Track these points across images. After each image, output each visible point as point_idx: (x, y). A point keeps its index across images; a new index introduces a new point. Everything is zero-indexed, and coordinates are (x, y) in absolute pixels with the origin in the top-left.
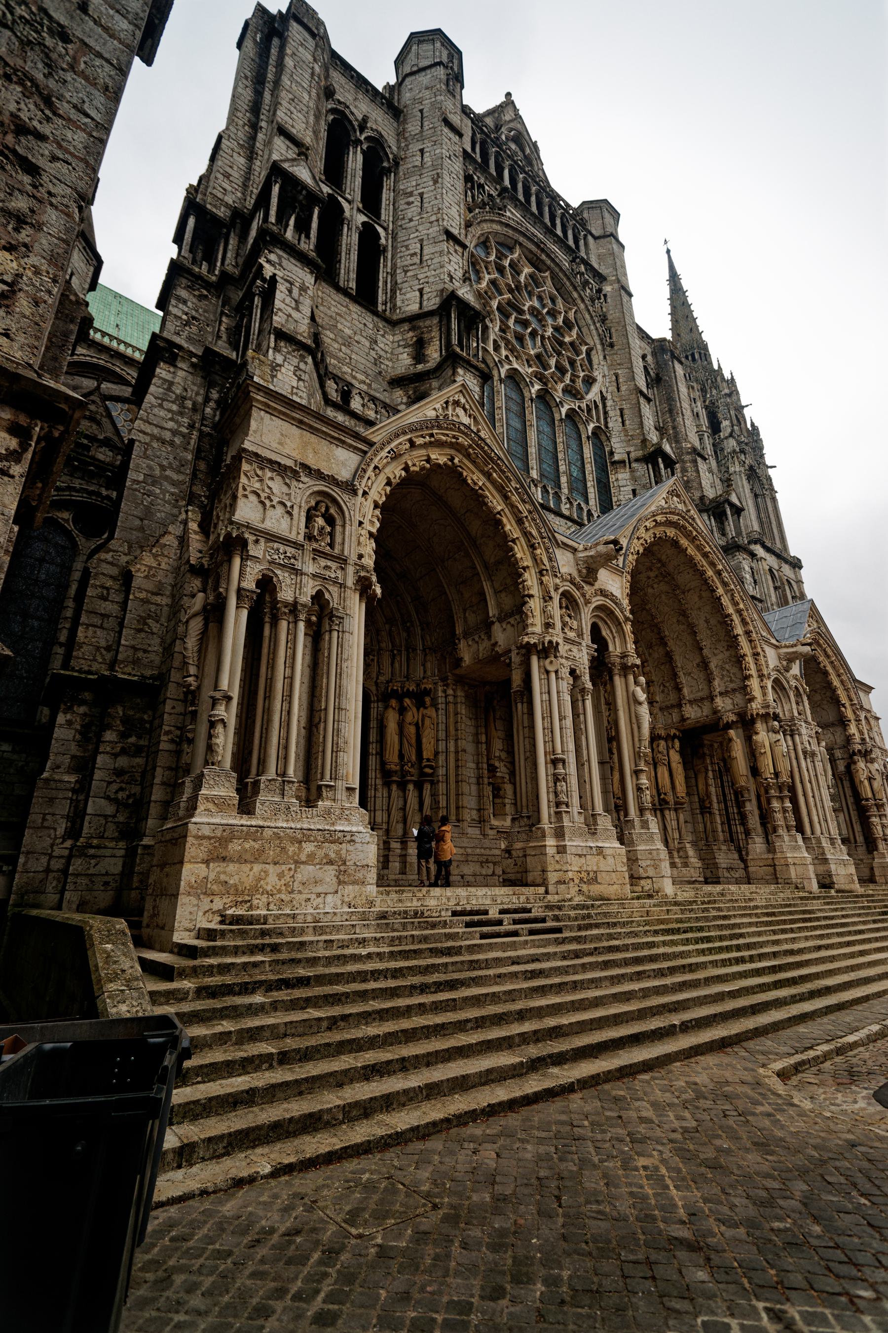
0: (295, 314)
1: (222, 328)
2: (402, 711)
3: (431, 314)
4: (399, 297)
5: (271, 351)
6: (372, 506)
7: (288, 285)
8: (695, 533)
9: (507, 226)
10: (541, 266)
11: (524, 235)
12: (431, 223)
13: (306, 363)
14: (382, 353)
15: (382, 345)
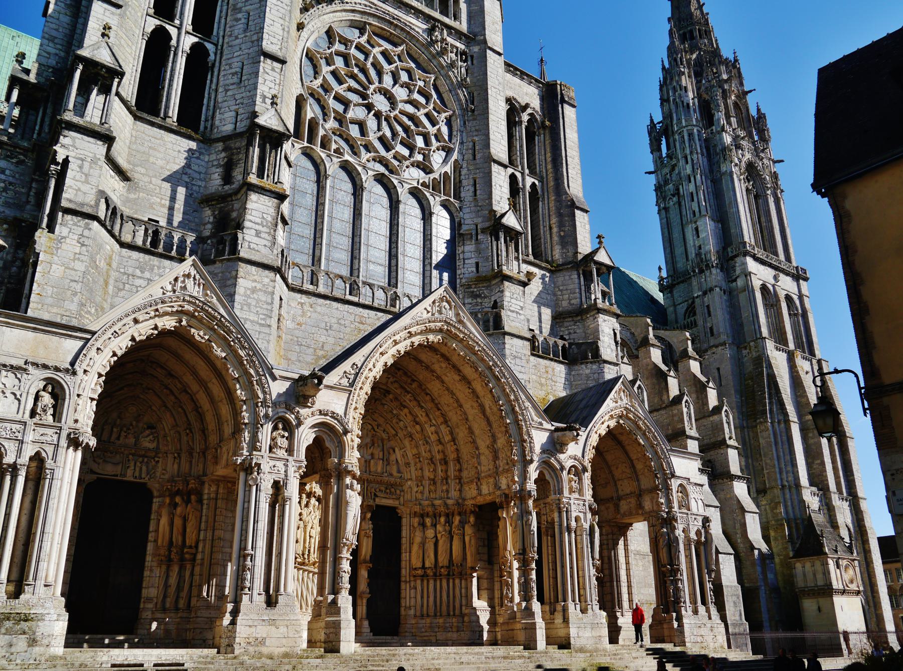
0: (85, 188)
1: (32, 193)
2: (175, 505)
3: (241, 135)
4: (218, 116)
5: (58, 226)
6: (97, 376)
7: (80, 162)
8: (462, 336)
9: (353, 11)
10: (396, 40)
11: (374, 16)
12: (252, 42)
13: (90, 229)
14: (196, 176)
15: (195, 167)
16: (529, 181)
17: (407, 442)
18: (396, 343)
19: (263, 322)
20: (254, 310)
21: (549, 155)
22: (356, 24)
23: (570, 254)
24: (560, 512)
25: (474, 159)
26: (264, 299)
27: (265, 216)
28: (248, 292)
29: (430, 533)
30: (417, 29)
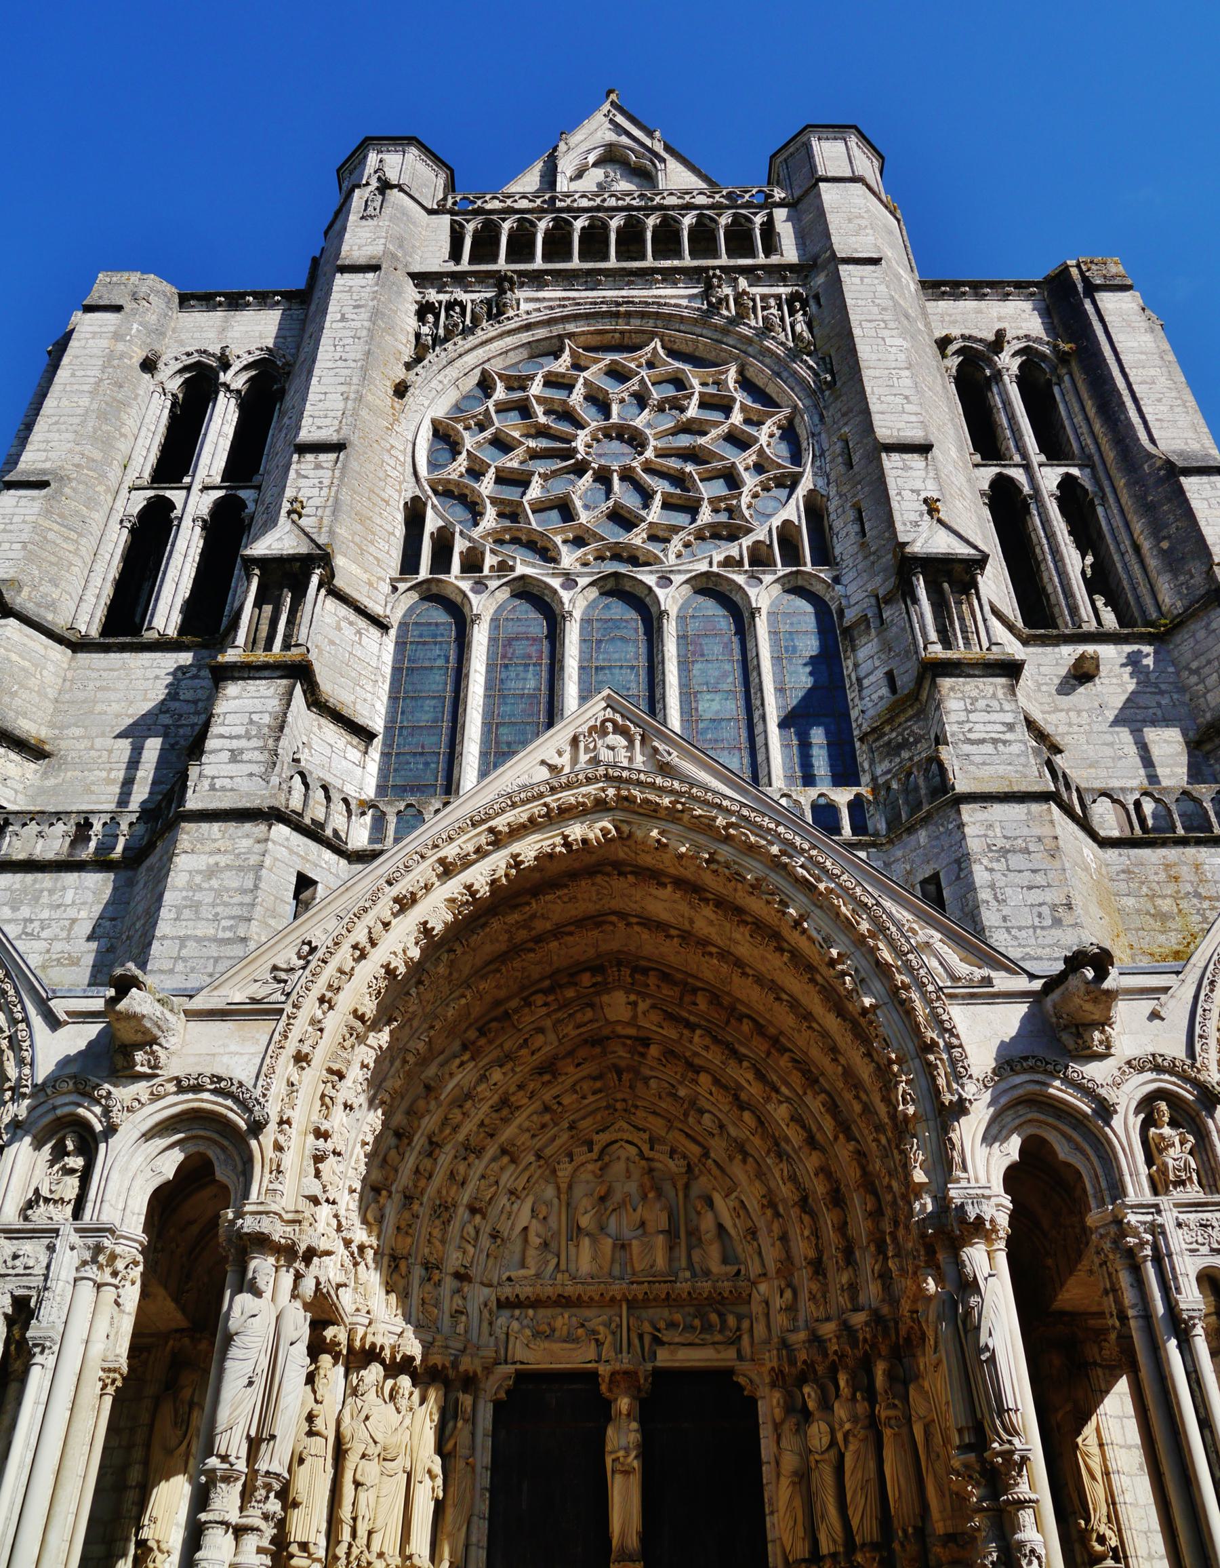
8: (666, 801)
9: (528, 327)
10: (637, 339)
11: (575, 317)
14: (187, 708)
16: (1050, 478)
17: (738, 1171)
18: (447, 870)
19: (228, 935)
20: (206, 912)
21: (1089, 404)
22: (545, 346)
23: (1198, 580)
24: (1136, 1270)
25: (850, 465)
26: (235, 884)
27: (255, 717)
28: (198, 879)
29: (818, 1434)
30: (673, 301)
